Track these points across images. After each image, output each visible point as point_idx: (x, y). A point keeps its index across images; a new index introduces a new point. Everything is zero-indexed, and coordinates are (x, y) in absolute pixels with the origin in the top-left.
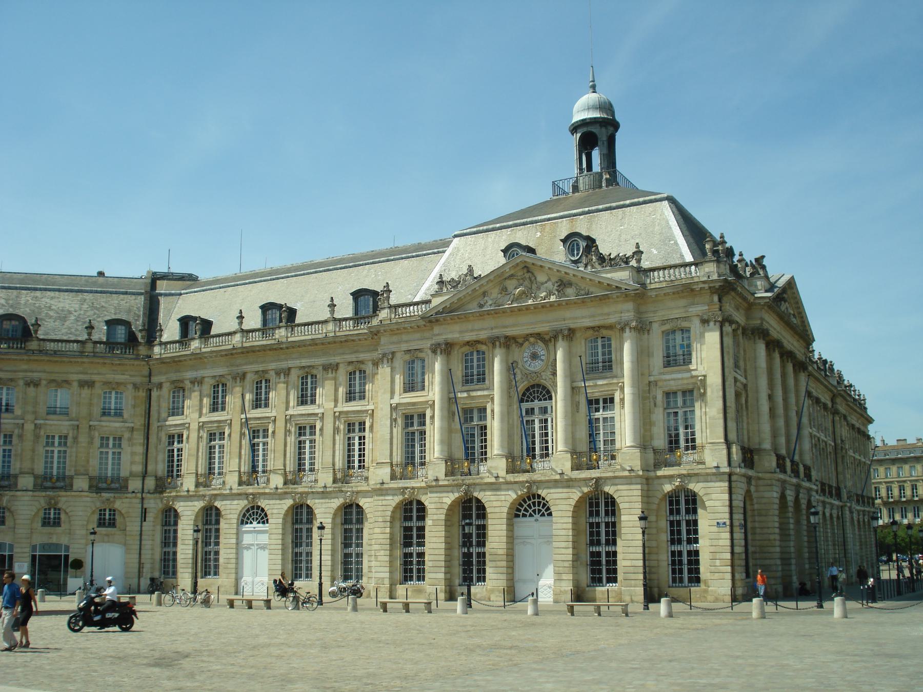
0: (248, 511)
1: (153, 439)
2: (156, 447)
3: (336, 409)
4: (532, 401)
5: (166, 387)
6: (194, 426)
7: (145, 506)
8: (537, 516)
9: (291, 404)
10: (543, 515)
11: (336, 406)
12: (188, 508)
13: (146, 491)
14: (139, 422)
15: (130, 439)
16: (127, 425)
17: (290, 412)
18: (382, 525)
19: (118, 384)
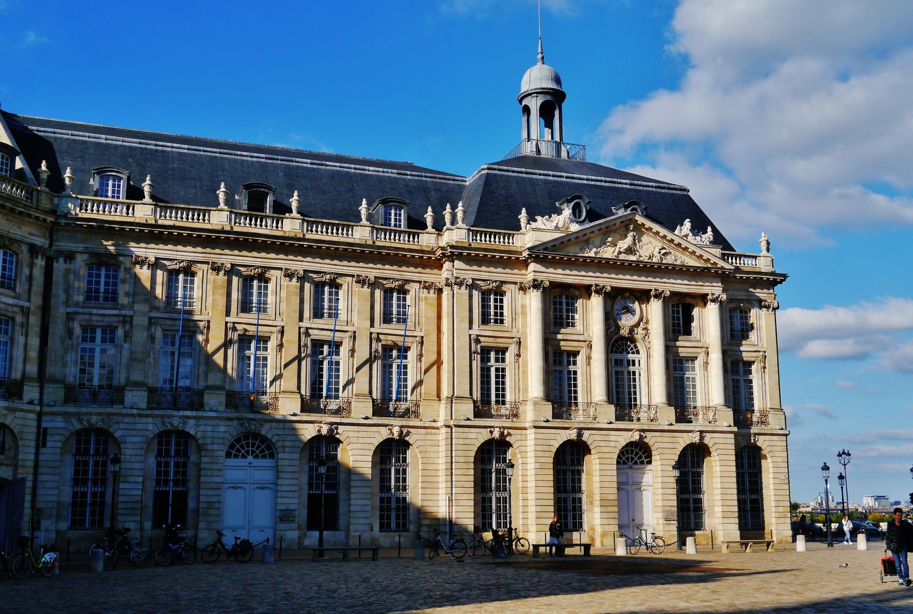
0: (238, 440)
1: (57, 330)
2: (63, 342)
3: (372, 330)
4: (621, 353)
5: (81, 259)
6: (140, 321)
7: (44, 425)
8: (630, 463)
9: (307, 314)
10: (636, 463)
11: (372, 325)
12: (135, 433)
13: (45, 401)
14: (37, 300)
15: (22, 325)
16: (22, 303)
17: (306, 324)
18: (464, 466)
19: (13, 241)
